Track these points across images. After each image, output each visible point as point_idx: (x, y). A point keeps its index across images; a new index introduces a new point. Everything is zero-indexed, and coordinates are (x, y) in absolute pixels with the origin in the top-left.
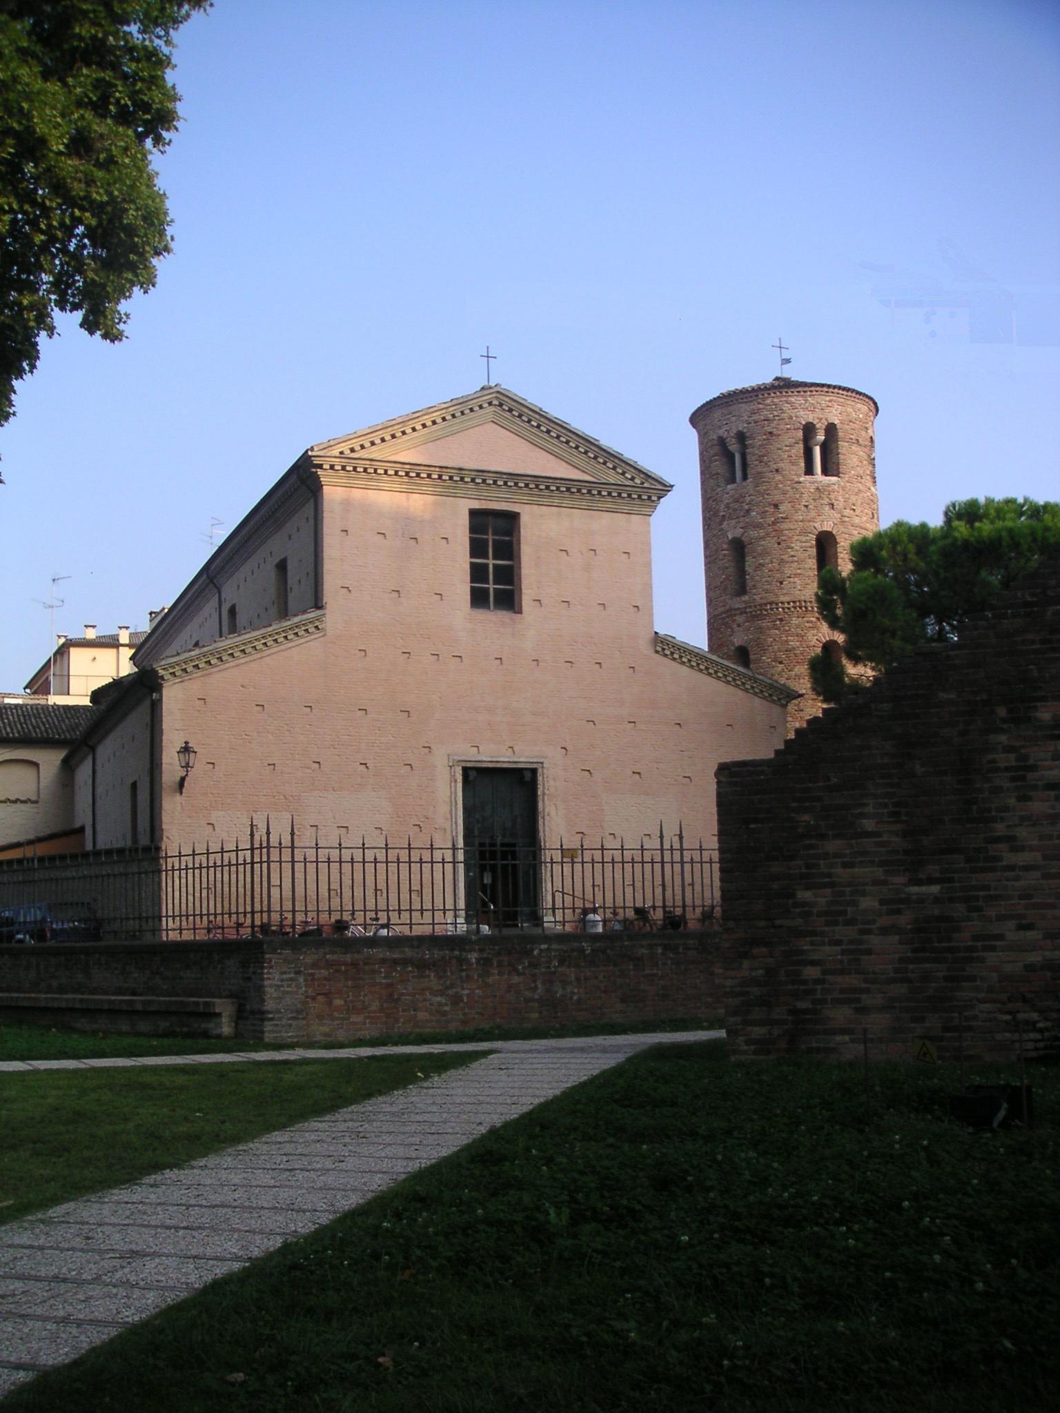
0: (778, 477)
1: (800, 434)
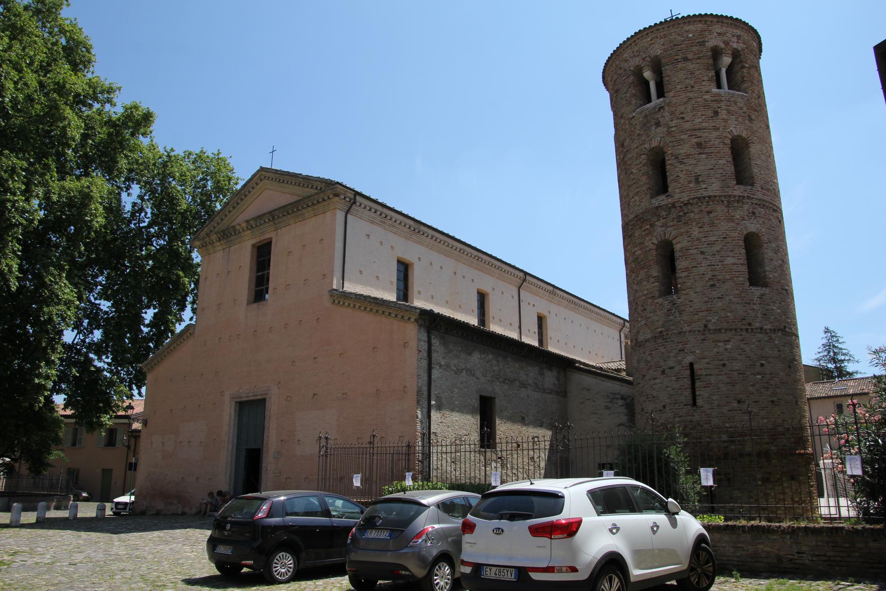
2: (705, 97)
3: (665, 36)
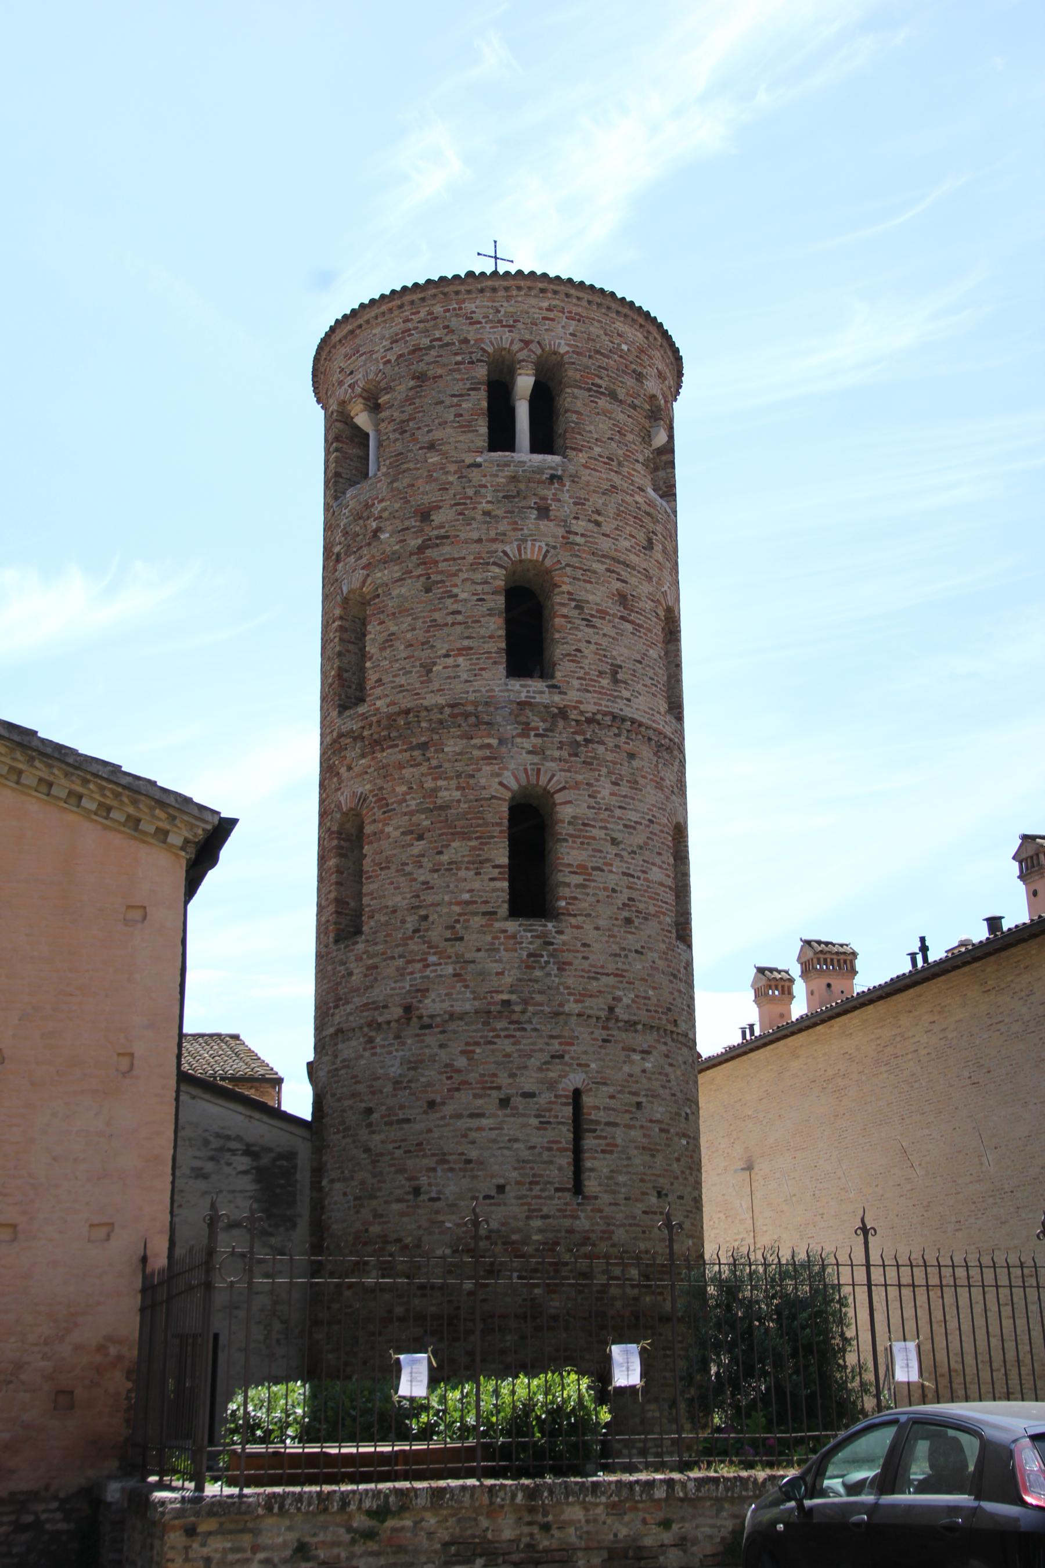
0: (434, 459)
1: (481, 372)
2: (638, 498)
3: (579, 319)
